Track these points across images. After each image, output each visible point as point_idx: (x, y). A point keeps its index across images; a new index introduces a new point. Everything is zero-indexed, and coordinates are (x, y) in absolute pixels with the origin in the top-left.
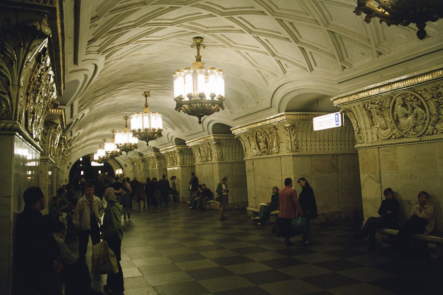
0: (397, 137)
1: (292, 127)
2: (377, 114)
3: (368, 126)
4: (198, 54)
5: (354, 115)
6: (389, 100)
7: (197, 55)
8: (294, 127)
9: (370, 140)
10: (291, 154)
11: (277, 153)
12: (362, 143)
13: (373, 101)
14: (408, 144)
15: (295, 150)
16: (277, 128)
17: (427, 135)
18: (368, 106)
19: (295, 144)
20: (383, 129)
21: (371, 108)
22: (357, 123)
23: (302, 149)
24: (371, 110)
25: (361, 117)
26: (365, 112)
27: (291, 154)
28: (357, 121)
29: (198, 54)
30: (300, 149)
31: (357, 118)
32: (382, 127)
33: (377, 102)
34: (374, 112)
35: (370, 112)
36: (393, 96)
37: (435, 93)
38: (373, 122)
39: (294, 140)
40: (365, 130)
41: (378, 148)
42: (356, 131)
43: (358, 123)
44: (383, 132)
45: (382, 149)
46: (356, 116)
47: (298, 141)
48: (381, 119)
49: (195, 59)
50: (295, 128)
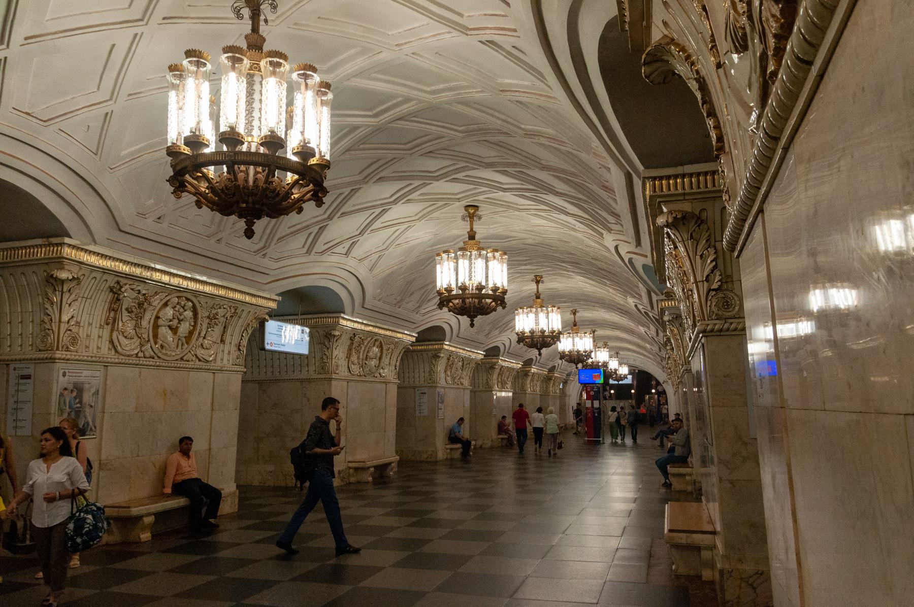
1: (692, 225)
15: (714, 309)
19: (715, 286)
39: (707, 271)
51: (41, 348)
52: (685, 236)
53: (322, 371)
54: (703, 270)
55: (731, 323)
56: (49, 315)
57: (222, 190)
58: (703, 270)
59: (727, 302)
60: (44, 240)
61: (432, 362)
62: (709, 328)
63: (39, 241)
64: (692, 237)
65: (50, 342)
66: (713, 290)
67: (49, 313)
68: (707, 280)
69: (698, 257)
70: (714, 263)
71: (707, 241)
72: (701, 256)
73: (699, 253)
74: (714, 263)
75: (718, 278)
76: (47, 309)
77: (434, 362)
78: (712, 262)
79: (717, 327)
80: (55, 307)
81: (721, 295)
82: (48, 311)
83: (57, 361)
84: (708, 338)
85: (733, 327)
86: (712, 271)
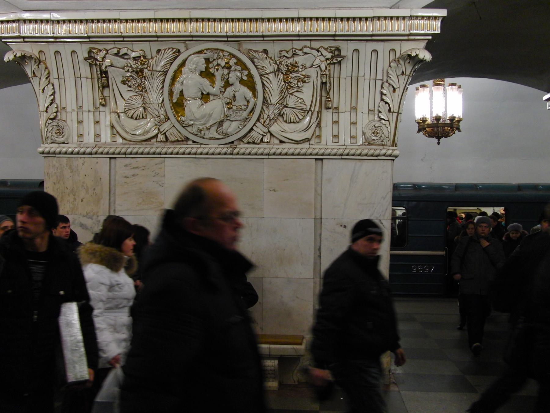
0: (172, 138)
2: (124, 82)
3: (87, 102)
5: (49, 73)
6: (169, 54)
9: (89, 139)
12: (64, 143)
13: (124, 51)
14: (197, 156)
17: (249, 143)
18: (103, 59)
20: (132, 117)
21: (111, 65)
22: (53, 94)
24: (110, 70)
25: (70, 83)
26: (85, 70)
28: (54, 89)
31: (56, 82)
32: (132, 112)
33: (133, 55)
34: (115, 76)
35: (104, 73)
36: (182, 49)
37: (284, 63)
38: (104, 98)
40: (75, 114)
41: (110, 158)
42: (46, 111)
43: (57, 96)
44: (130, 124)
45: (120, 163)
46: (54, 74)
48: (132, 94)
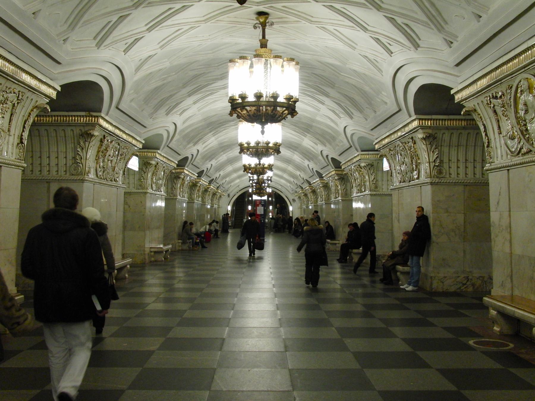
1: (431, 139)
4: (264, 36)
5: (481, 117)
7: (261, 37)
8: (436, 138)
10: (428, 180)
11: (418, 178)
15: (436, 174)
16: (415, 141)
19: (437, 164)
23: (450, 174)
27: (428, 181)
29: (264, 36)
30: (446, 173)
39: (434, 158)
46: (483, 119)
47: (441, 162)
49: (259, 44)
50: (435, 140)
51: (73, 174)
52: (428, 143)
53: (140, 187)
54: (433, 157)
55: (442, 180)
56: (80, 155)
57: (253, 115)
58: (433, 157)
59: (441, 171)
60: (87, 113)
61: (174, 182)
62: (434, 181)
63: (83, 113)
64: (430, 144)
65: (80, 170)
66: (436, 166)
67: (80, 154)
68: (434, 162)
69: (431, 152)
70: (437, 155)
71: (436, 146)
72: (433, 152)
73: (432, 150)
74: (437, 155)
75: (438, 161)
76: (79, 151)
77: (175, 181)
78: (437, 154)
79: (436, 181)
80: (84, 150)
81: (438, 168)
82: (78, 152)
83: (85, 181)
84: (433, 186)
85: (442, 181)
86: (436, 158)
